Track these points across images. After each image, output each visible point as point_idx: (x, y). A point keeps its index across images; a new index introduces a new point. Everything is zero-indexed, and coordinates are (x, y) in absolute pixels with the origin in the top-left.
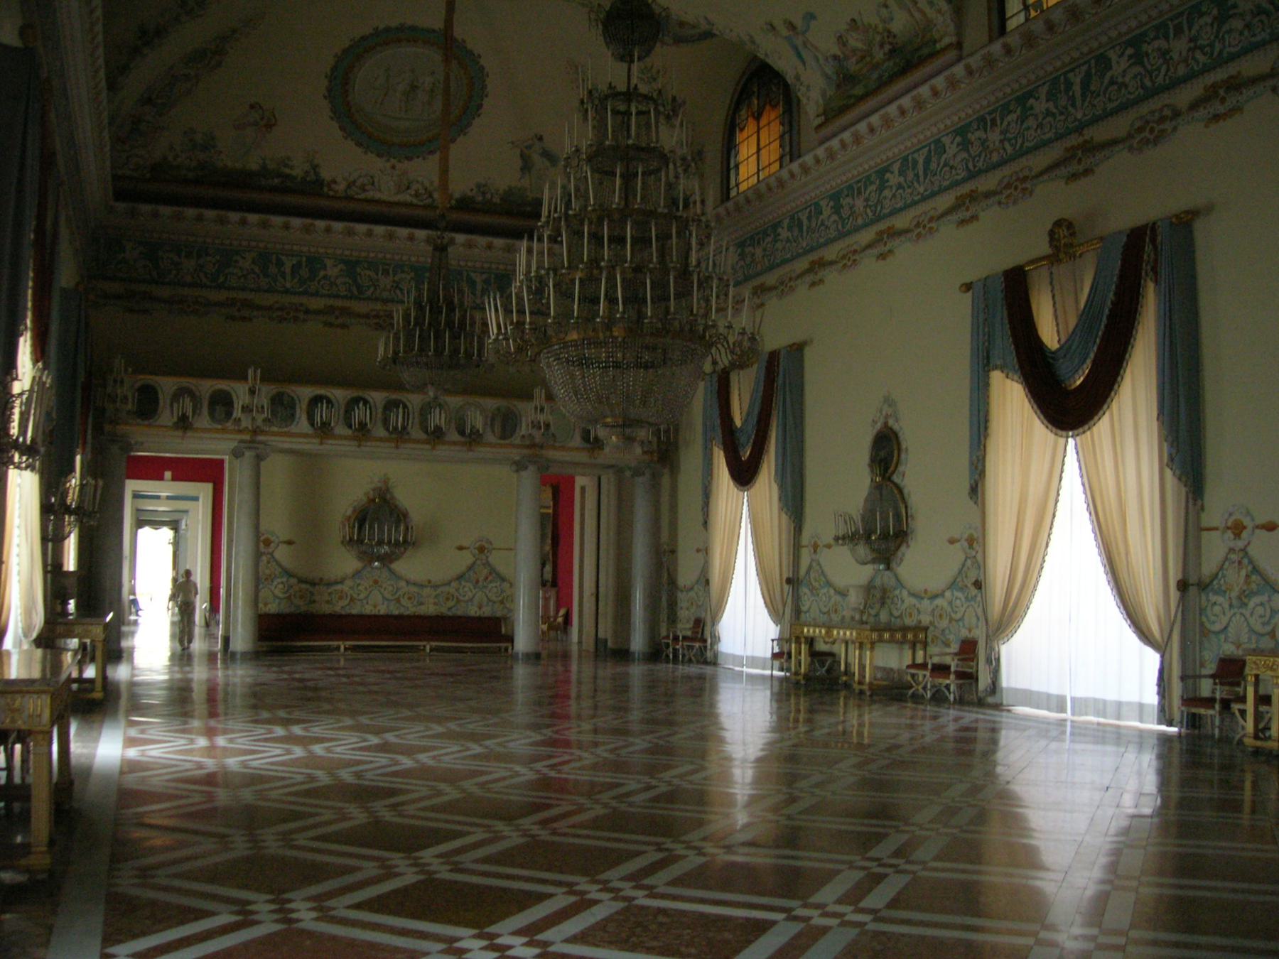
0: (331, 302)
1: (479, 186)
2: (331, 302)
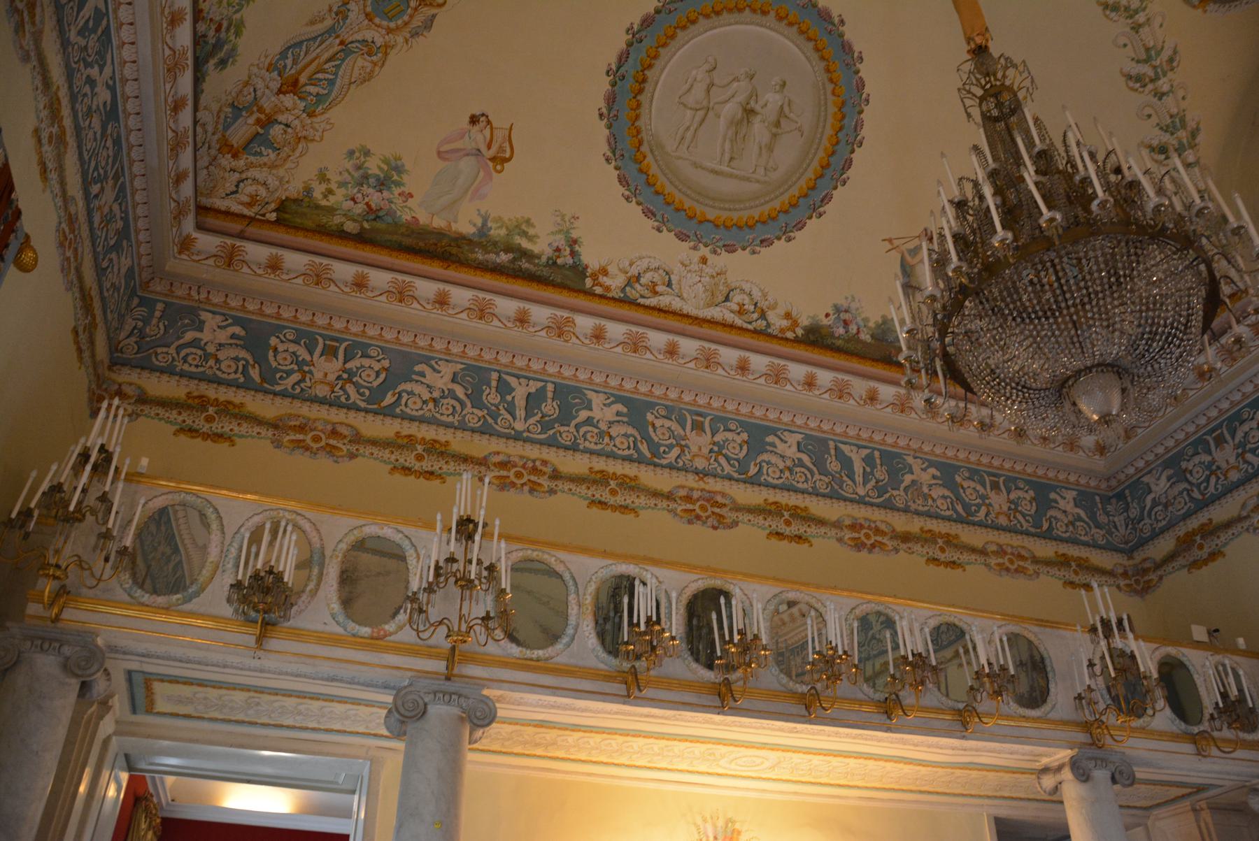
0: (600, 464)
1: (838, 309)
2: (600, 464)
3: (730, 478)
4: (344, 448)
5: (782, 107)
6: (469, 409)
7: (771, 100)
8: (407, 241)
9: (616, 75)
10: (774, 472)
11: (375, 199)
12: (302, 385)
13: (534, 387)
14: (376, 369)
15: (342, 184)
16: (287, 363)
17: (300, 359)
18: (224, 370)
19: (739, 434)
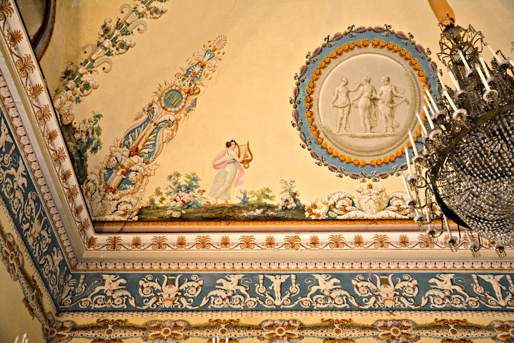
0: (328, 316)
2: (328, 316)
3: (410, 310)
4: (181, 334)
5: (391, 92)
6: (248, 298)
7: (384, 90)
8: (206, 215)
9: (295, 102)
10: (438, 300)
11: (186, 197)
12: (157, 303)
13: (284, 278)
14: (196, 286)
15: (169, 194)
16: (149, 293)
17: (155, 289)
18: (116, 303)
19: (411, 281)
